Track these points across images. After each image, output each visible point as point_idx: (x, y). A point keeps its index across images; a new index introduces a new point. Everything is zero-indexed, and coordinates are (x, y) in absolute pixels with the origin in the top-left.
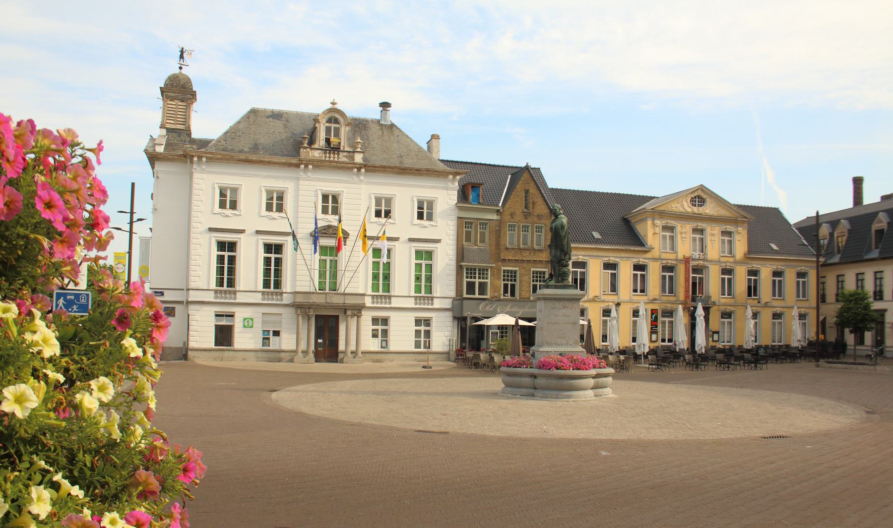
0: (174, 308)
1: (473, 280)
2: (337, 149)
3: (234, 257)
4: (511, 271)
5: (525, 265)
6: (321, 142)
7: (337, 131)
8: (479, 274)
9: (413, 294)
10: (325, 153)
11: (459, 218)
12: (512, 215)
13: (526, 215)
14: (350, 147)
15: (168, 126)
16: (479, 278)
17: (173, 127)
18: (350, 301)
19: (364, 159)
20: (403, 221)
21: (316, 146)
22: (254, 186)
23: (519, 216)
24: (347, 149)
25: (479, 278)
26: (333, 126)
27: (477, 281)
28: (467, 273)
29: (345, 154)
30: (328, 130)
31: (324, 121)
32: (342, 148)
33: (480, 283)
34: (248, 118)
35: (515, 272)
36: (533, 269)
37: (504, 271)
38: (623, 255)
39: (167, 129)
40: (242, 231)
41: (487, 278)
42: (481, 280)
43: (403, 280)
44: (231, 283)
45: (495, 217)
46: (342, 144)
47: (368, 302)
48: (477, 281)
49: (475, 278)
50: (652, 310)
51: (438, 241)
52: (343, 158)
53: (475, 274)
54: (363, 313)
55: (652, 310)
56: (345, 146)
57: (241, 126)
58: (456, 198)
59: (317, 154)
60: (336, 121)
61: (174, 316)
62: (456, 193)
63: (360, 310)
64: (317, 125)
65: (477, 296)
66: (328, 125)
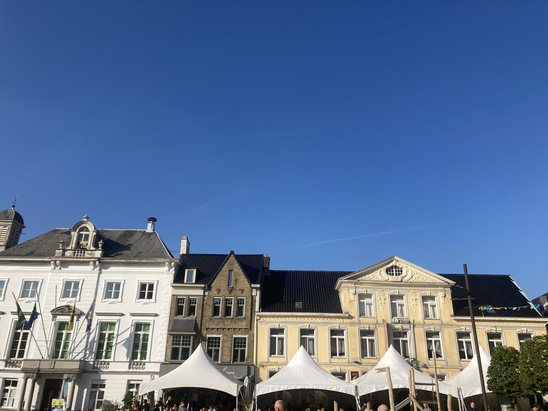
4: (216, 338)
8: (183, 341)
16: (183, 344)
25: (183, 344)
27: (181, 347)
29: (90, 252)
33: (183, 348)
35: (219, 338)
36: (234, 336)
38: (318, 320)
41: (189, 345)
45: (201, 292)
46: (89, 245)
48: (181, 347)
49: (179, 344)
50: (352, 372)
53: (180, 341)
55: (352, 372)
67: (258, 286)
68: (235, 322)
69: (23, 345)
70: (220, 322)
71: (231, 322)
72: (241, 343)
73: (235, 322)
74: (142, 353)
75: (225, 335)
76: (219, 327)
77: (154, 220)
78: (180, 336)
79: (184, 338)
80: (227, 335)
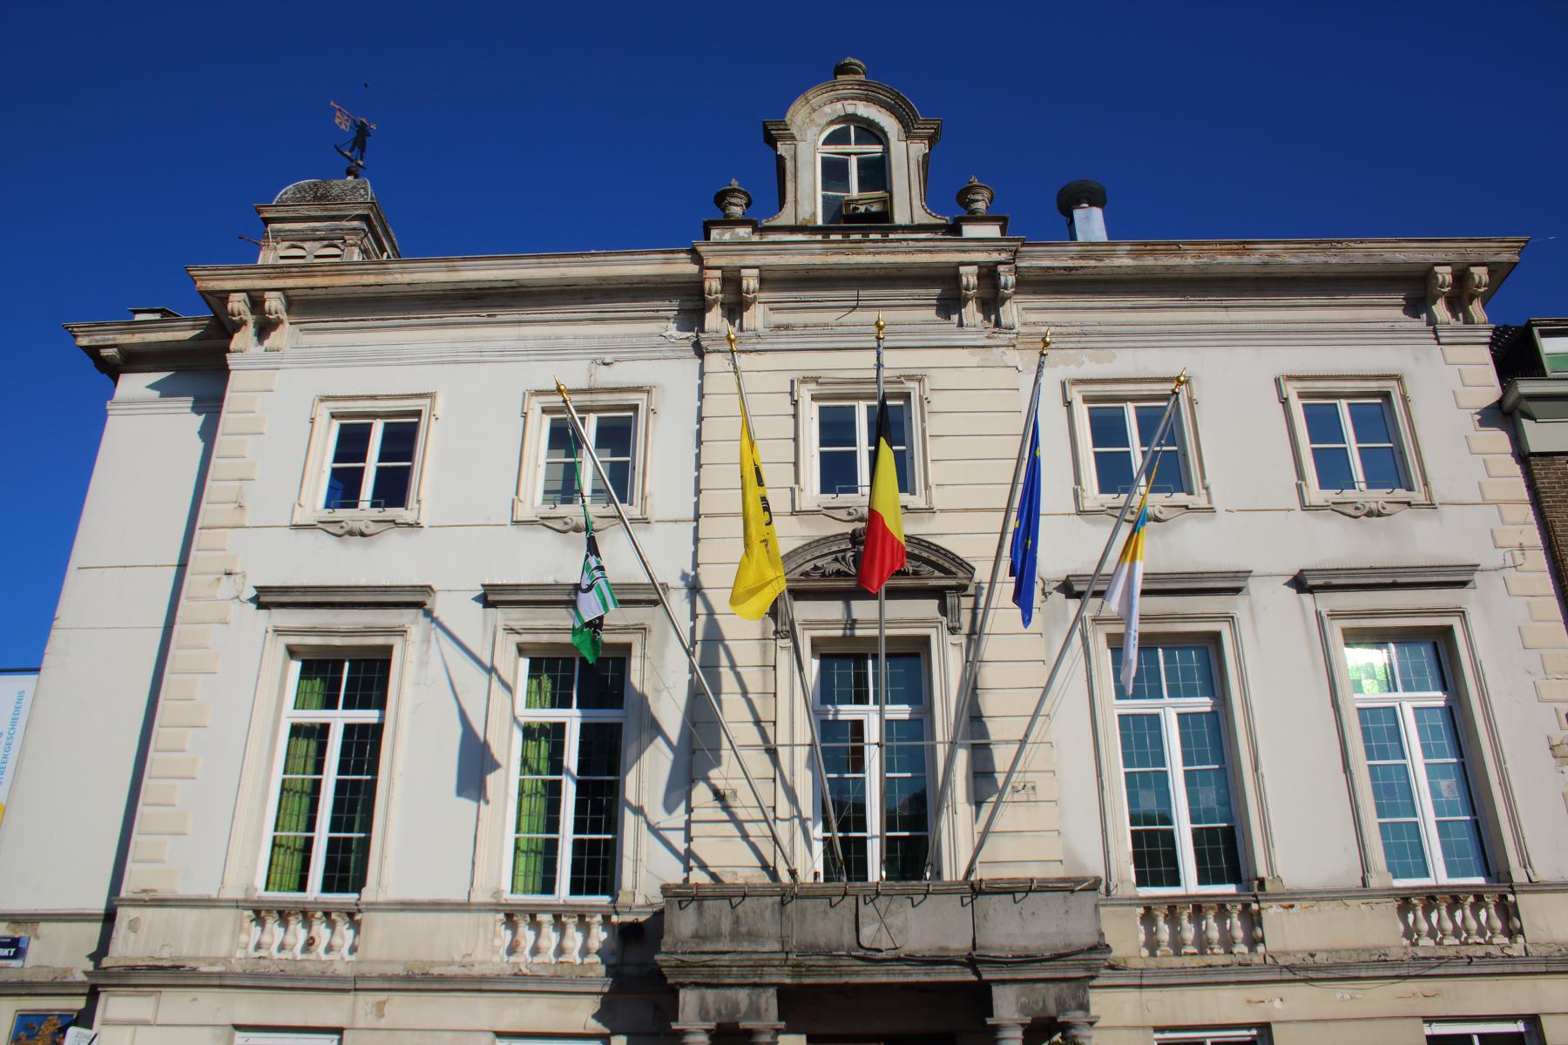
3: (378, 729)
9: (1381, 877)
14: (931, 199)
18: (1008, 930)
20: (1251, 505)
21: (786, 218)
24: (922, 217)
30: (834, 172)
32: (901, 217)
40: (416, 600)
44: (347, 868)
47: (1125, 937)
51: (1456, 578)
54: (1099, 1001)
60: (870, 132)
62: (1485, 354)
63: (1084, 983)
64: (783, 149)
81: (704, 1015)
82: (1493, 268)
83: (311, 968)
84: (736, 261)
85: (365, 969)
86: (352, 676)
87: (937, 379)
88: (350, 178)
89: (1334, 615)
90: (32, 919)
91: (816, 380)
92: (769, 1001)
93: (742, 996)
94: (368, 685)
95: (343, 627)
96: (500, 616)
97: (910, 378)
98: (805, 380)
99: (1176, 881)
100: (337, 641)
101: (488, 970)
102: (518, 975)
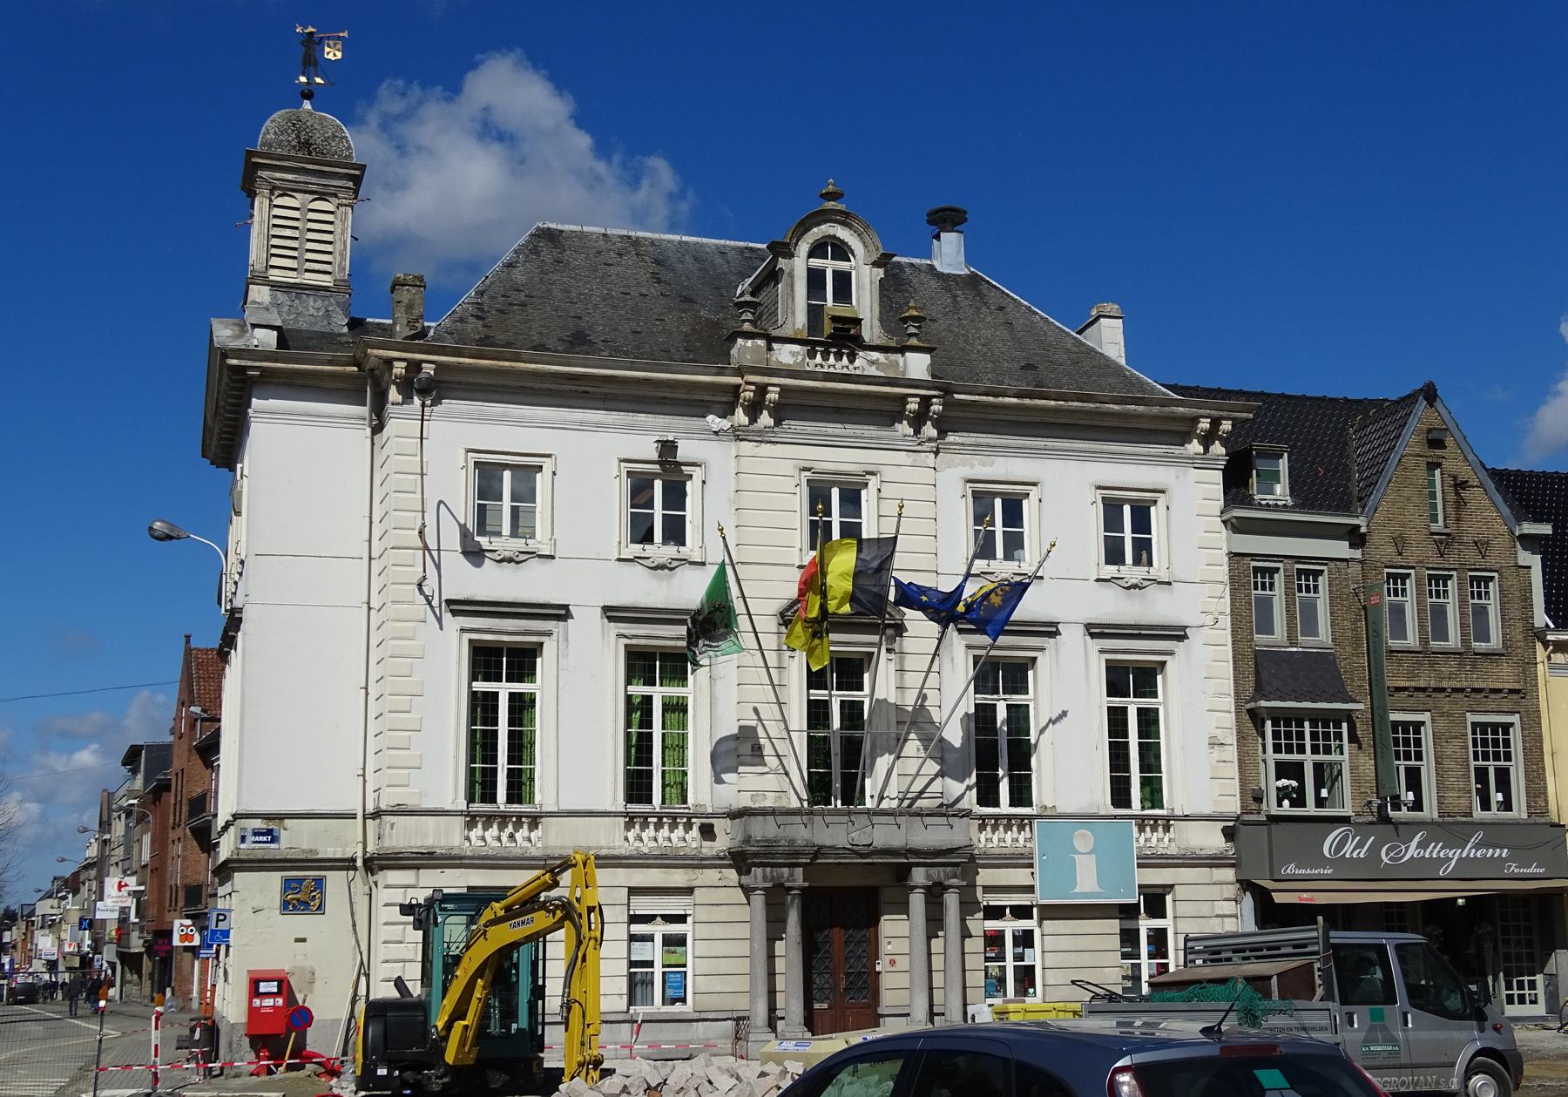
0: (319, 883)
1: (1295, 757)
2: (845, 337)
5: (1444, 702)
6: (795, 313)
7: (843, 280)
8: (1314, 736)
10: (812, 355)
11: (1234, 556)
12: (1400, 542)
13: (1444, 542)
15: (275, 275)
16: (1315, 750)
17: (291, 278)
19: (934, 370)
22: (585, 458)
23: (1421, 551)
26: (830, 266)
27: (1309, 759)
28: (1276, 735)
29: (875, 355)
30: (815, 279)
31: (804, 248)
34: (535, 251)
36: (1471, 718)
37: (1395, 724)
39: (276, 286)
40: (561, 613)
42: (1321, 757)
43: (1070, 767)
45: (1341, 549)
48: (1309, 759)
49: (1301, 750)
51: (1178, 634)
52: (865, 363)
53: (1301, 736)
56: (871, 330)
57: (518, 275)
58: (1218, 490)
59: (786, 355)
60: (842, 251)
61: (321, 908)
62: (1218, 476)
65: (1311, 809)
66: (816, 262)
67: (1546, 529)
68: (1474, 666)
69: (520, 746)
70: (1420, 664)
71: (1461, 665)
72: (1485, 743)
73: (1474, 666)
74: (1013, 780)
75: (1442, 714)
76: (1422, 684)
77: (947, 219)
78: (1298, 717)
79: (1314, 724)
80: (1448, 714)
81: (765, 879)
82: (1235, 421)
83: (517, 852)
84: (766, 380)
85: (549, 852)
86: (502, 660)
87: (888, 474)
88: (307, 105)
89: (1102, 651)
90: (280, 817)
91: (808, 470)
92: (799, 871)
93: (786, 870)
94: (521, 666)
95: (510, 629)
96: (615, 628)
97: (869, 473)
98: (805, 469)
99: (997, 804)
100: (506, 638)
101: (623, 852)
102: (645, 856)
